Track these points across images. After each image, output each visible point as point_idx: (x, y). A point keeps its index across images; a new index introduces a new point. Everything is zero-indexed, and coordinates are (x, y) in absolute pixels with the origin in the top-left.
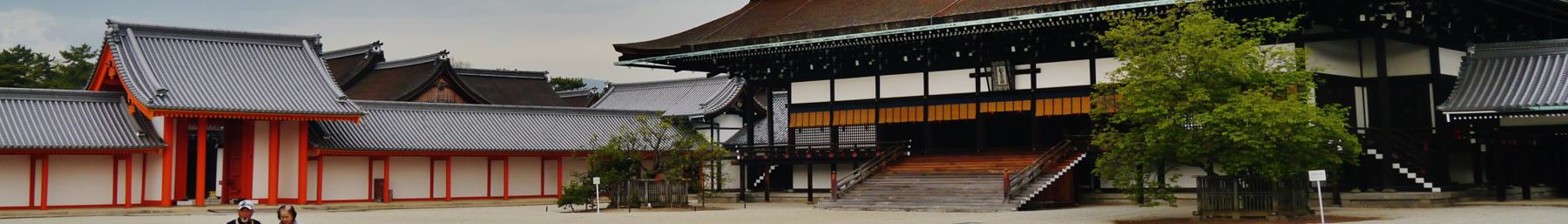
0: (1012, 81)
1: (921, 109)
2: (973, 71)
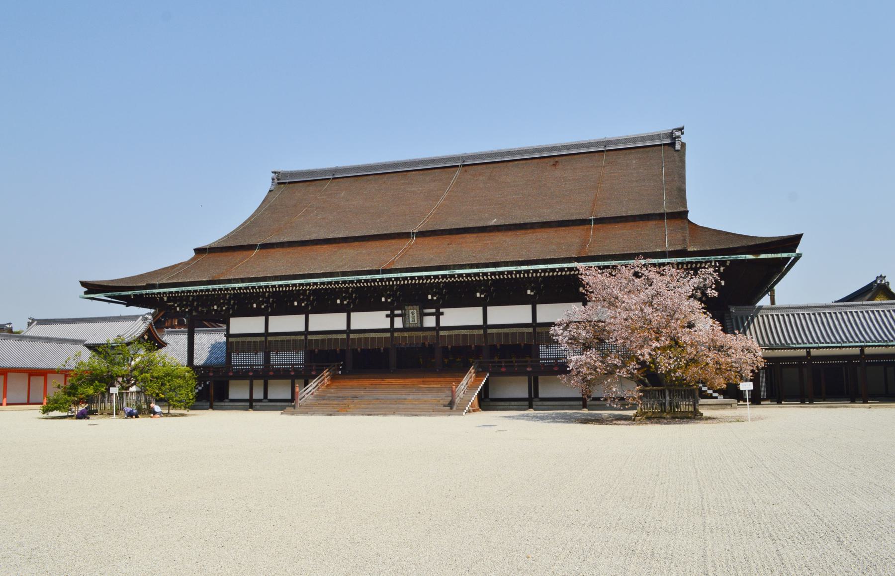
0: (422, 322)
2: (388, 312)
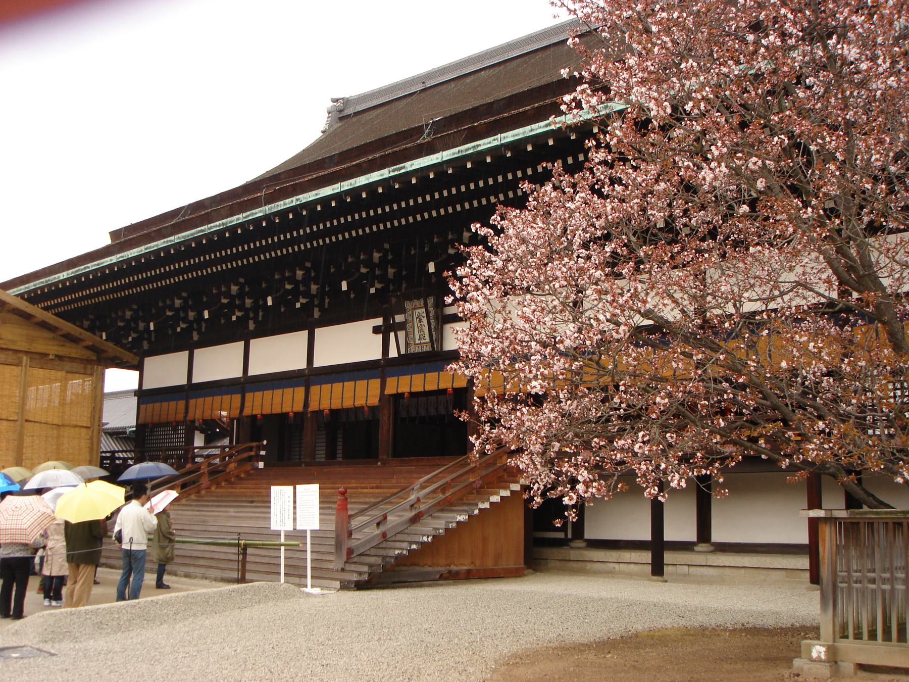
0: (437, 336)
1: (300, 392)
2: (379, 321)
